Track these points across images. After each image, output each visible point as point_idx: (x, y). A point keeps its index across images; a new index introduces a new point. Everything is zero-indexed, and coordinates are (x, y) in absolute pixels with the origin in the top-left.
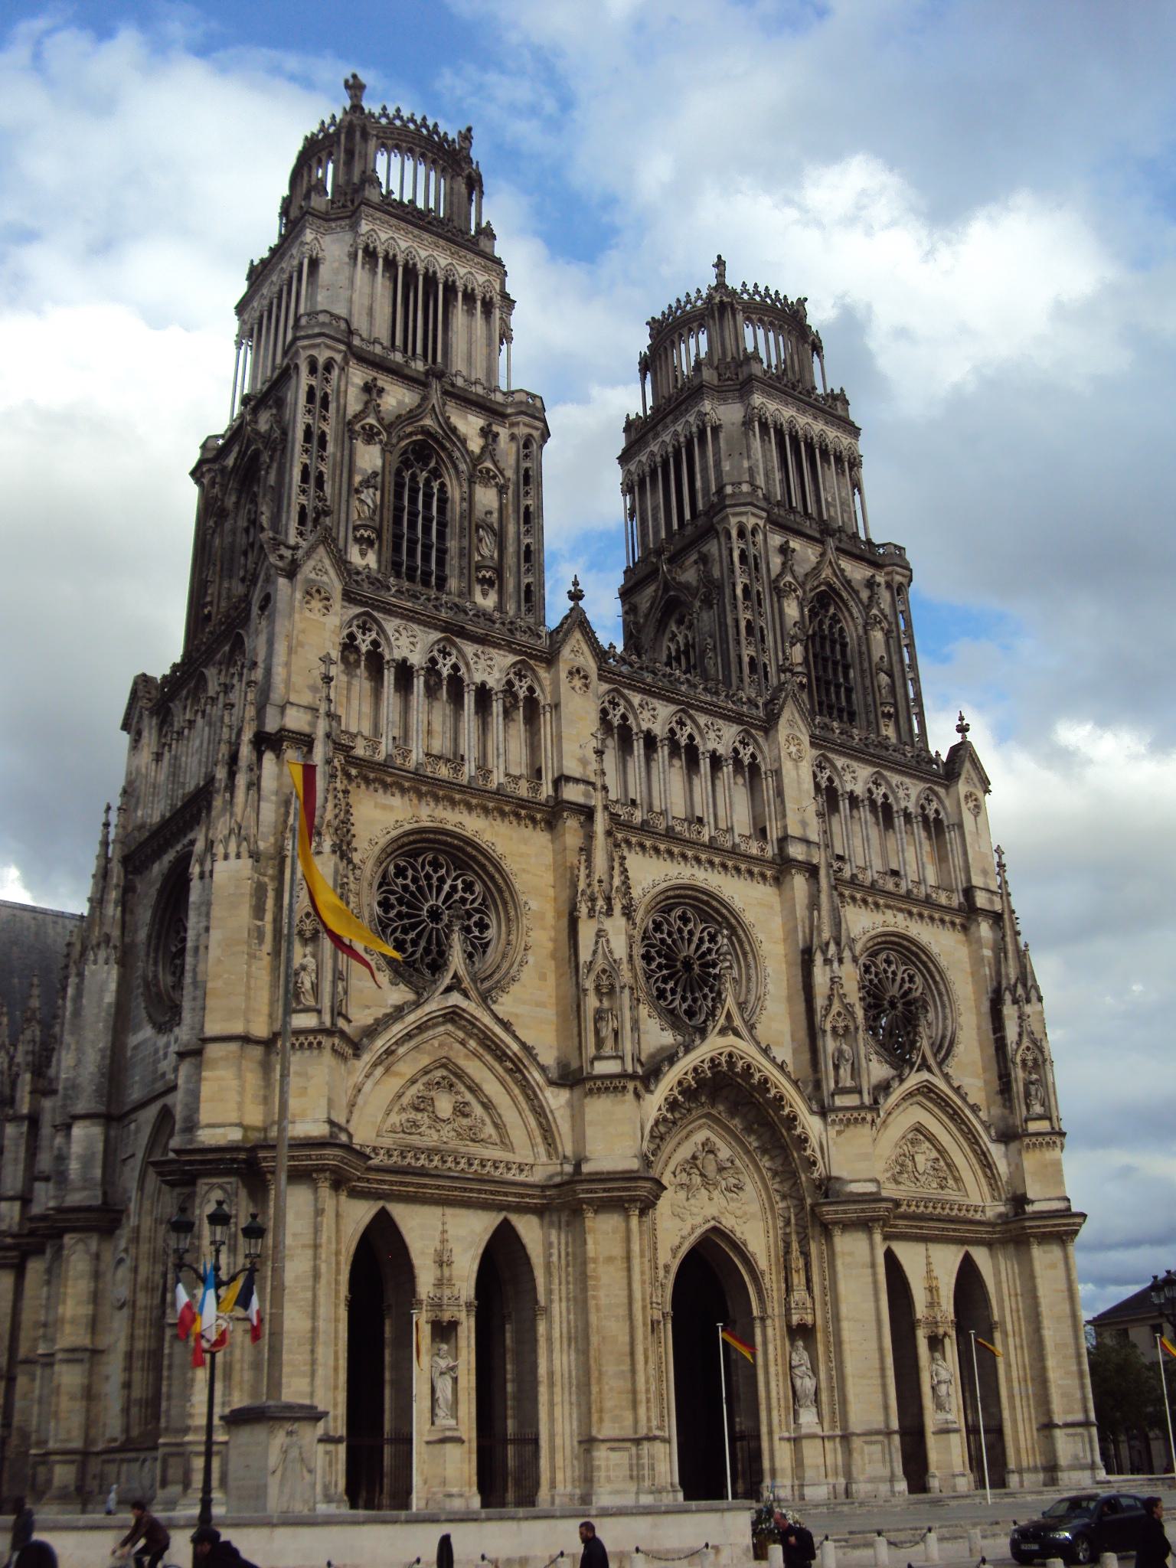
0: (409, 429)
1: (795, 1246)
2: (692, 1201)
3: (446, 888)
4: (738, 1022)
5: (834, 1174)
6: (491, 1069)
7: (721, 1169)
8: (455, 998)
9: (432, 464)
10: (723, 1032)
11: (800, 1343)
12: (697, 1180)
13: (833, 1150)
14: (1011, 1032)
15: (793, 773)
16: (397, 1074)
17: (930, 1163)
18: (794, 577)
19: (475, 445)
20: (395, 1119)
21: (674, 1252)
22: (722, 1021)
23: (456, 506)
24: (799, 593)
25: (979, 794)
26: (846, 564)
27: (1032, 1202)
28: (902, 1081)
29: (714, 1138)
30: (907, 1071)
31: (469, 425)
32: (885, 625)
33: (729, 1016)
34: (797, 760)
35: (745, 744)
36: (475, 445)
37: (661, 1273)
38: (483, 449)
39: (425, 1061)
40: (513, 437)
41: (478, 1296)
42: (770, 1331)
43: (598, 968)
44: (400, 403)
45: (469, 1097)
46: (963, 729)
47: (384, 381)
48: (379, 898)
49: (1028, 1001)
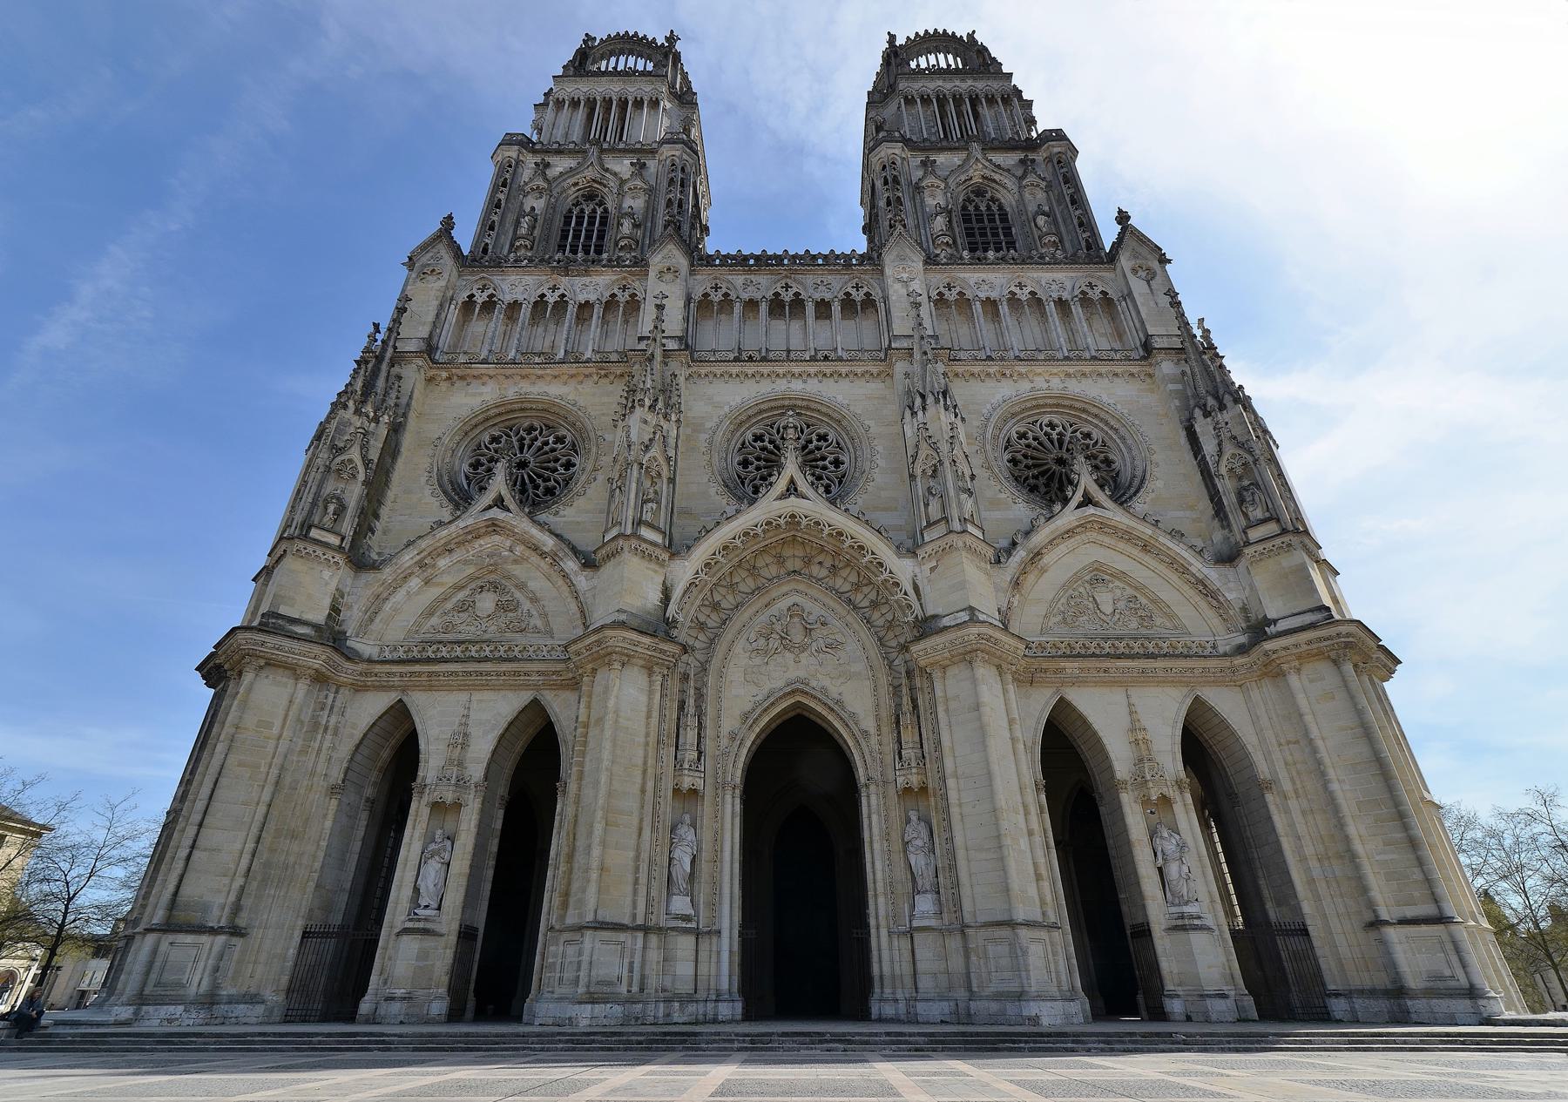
0: (571, 181)
1: (906, 700)
2: (771, 667)
3: (538, 443)
4: (803, 486)
5: (930, 612)
6: (538, 568)
7: (808, 631)
8: (496, 513)
11: (913, 816)
12: (775, 643)
13: (925, 588)
14: (1209, 447)
16: (439, 584)
17: (1121, 605)
22: (781, 485)
25: (1155, 265)
27: (1275, 621)
29: (808, 605)
30: (1057, 507)
33: (792, 481)
35: (857, 288)
37: (725, 742)
39: (471, 570)
41: (486, 777)
42: (873, 798)
43: (621, 458)
45: (518, 595)
46: (1123, 218)
47: (549, 159)
48: (473, 460)
49: (1222, 407)
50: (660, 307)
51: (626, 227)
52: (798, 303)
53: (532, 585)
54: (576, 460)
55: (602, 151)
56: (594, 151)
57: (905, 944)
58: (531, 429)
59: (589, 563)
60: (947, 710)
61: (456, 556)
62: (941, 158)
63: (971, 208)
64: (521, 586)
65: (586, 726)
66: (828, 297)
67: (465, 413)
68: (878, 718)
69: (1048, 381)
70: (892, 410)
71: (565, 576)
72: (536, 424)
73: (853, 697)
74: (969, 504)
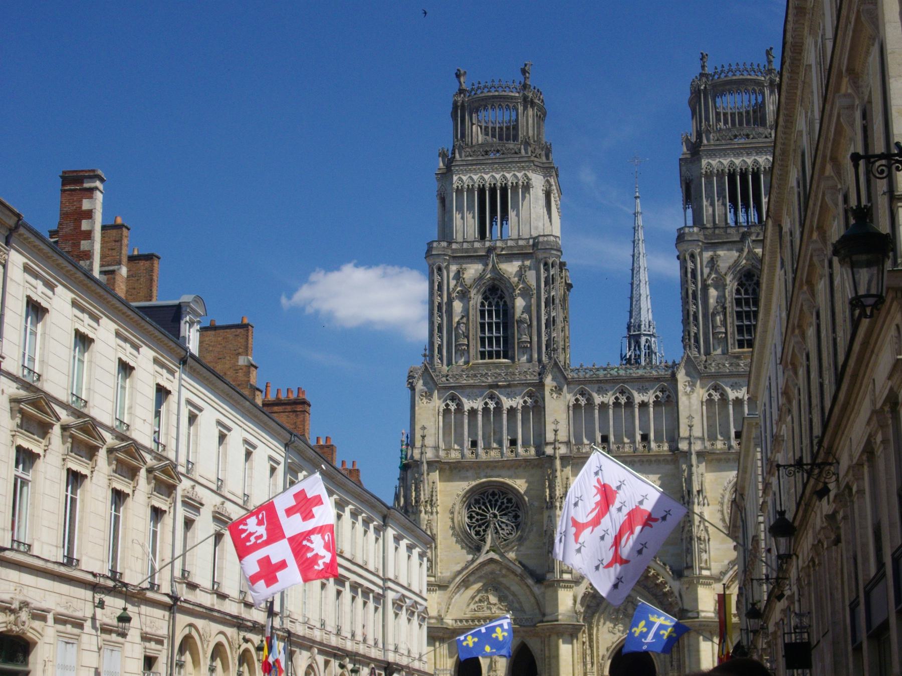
3: (499, 503)
5: (686, 607)
9: (499, 292)
13: (684, 597)
15: (687, 402)
20: (473, 606)
21: (608, 650)
31: (511, 268)
37: (600, 658)
44: (476, 270)
45: (506, 592)
50: (556, 431)
53: (512, 588)
54: (519, 513)
58: (493, 494)
59: (540, 579)
60: (689, 650)
61: (477, 576)
64: (508, 589)
65: (549, 658)
67: (462, 493)
71: (528, 586)
72: (496, 491)
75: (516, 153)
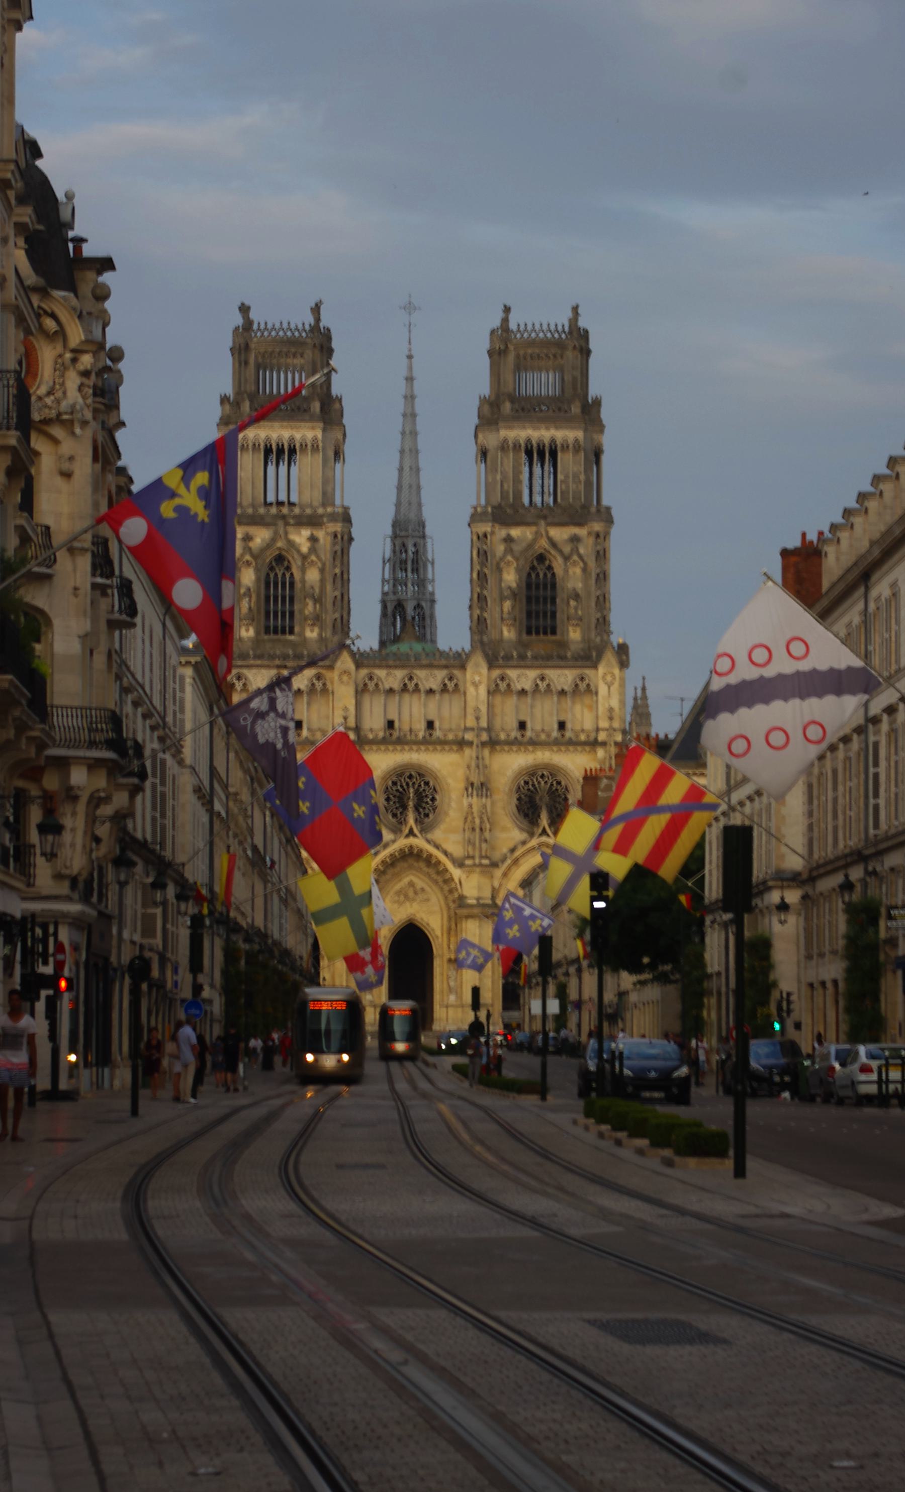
1: (453, 926)
4: (416, 831)
7: (416, 893)
9: (286, 563)
10: (407, 836)
12: (402, 898)
18: (514, 557)
19: (305, 549)
22: (407, 831)
23: (298, 585)
24: (515, 565)
25: (616, 671)
26: (554, 532)
28: (524, 843)
29: (415, 880)
32: (581, 564)
34: (476, 685)
35: (451, 679)
36: (305, 549)
38: (310, 549)
40: (327, 534)
44: (263, 540)
47: (252, 530)
51: (310, 608)
52: (417, 689)
55: (287, 524)
56: (281, 523)
57: (445, 1009)
62: (515, 532)
63: (533, 576)
66: (434, 687)
68: (442, 930)
69: (543, 756)
70: (461, 773)
73: (433, 922)
74: (484, 846)
75: (305, 411)
